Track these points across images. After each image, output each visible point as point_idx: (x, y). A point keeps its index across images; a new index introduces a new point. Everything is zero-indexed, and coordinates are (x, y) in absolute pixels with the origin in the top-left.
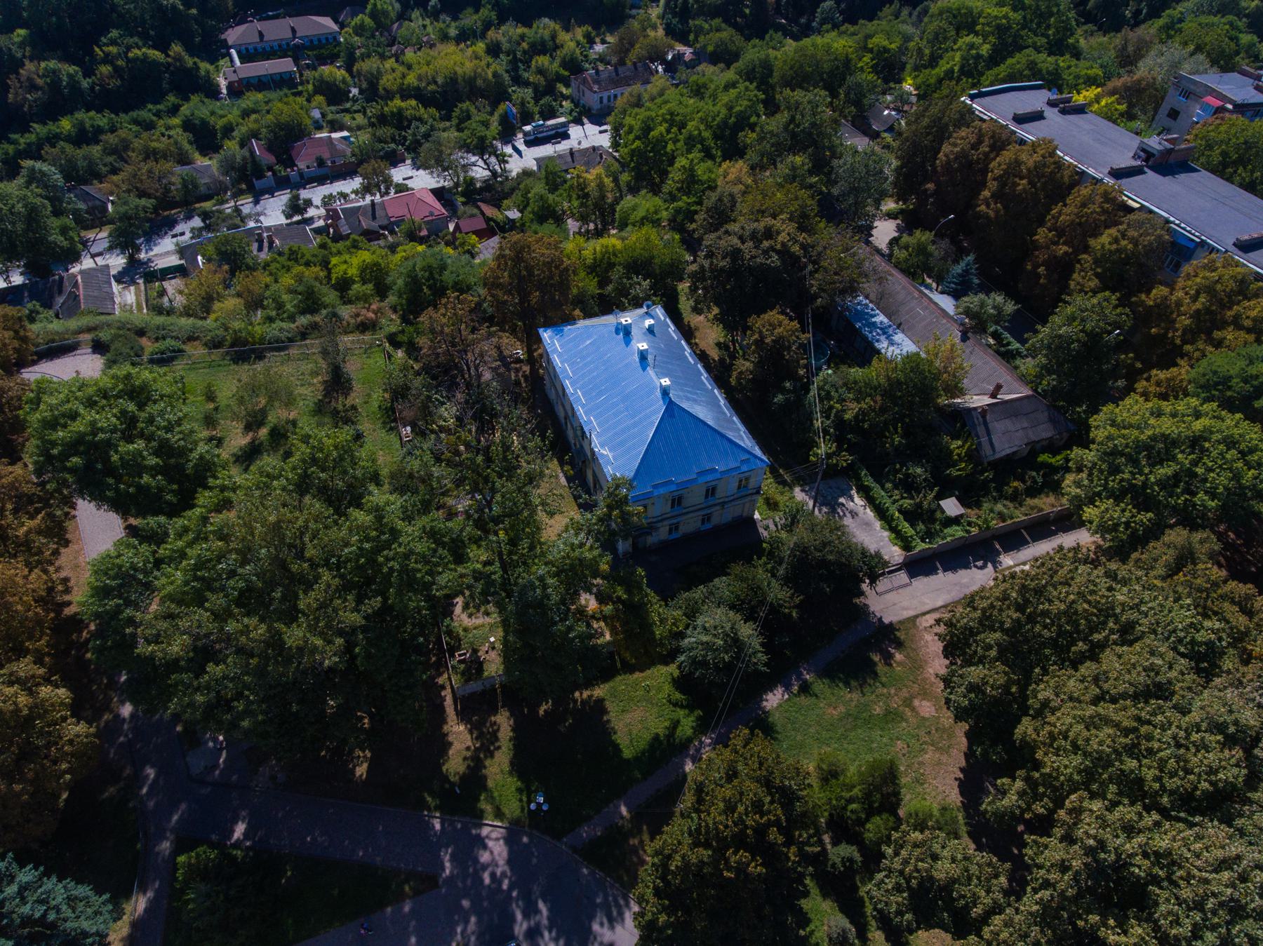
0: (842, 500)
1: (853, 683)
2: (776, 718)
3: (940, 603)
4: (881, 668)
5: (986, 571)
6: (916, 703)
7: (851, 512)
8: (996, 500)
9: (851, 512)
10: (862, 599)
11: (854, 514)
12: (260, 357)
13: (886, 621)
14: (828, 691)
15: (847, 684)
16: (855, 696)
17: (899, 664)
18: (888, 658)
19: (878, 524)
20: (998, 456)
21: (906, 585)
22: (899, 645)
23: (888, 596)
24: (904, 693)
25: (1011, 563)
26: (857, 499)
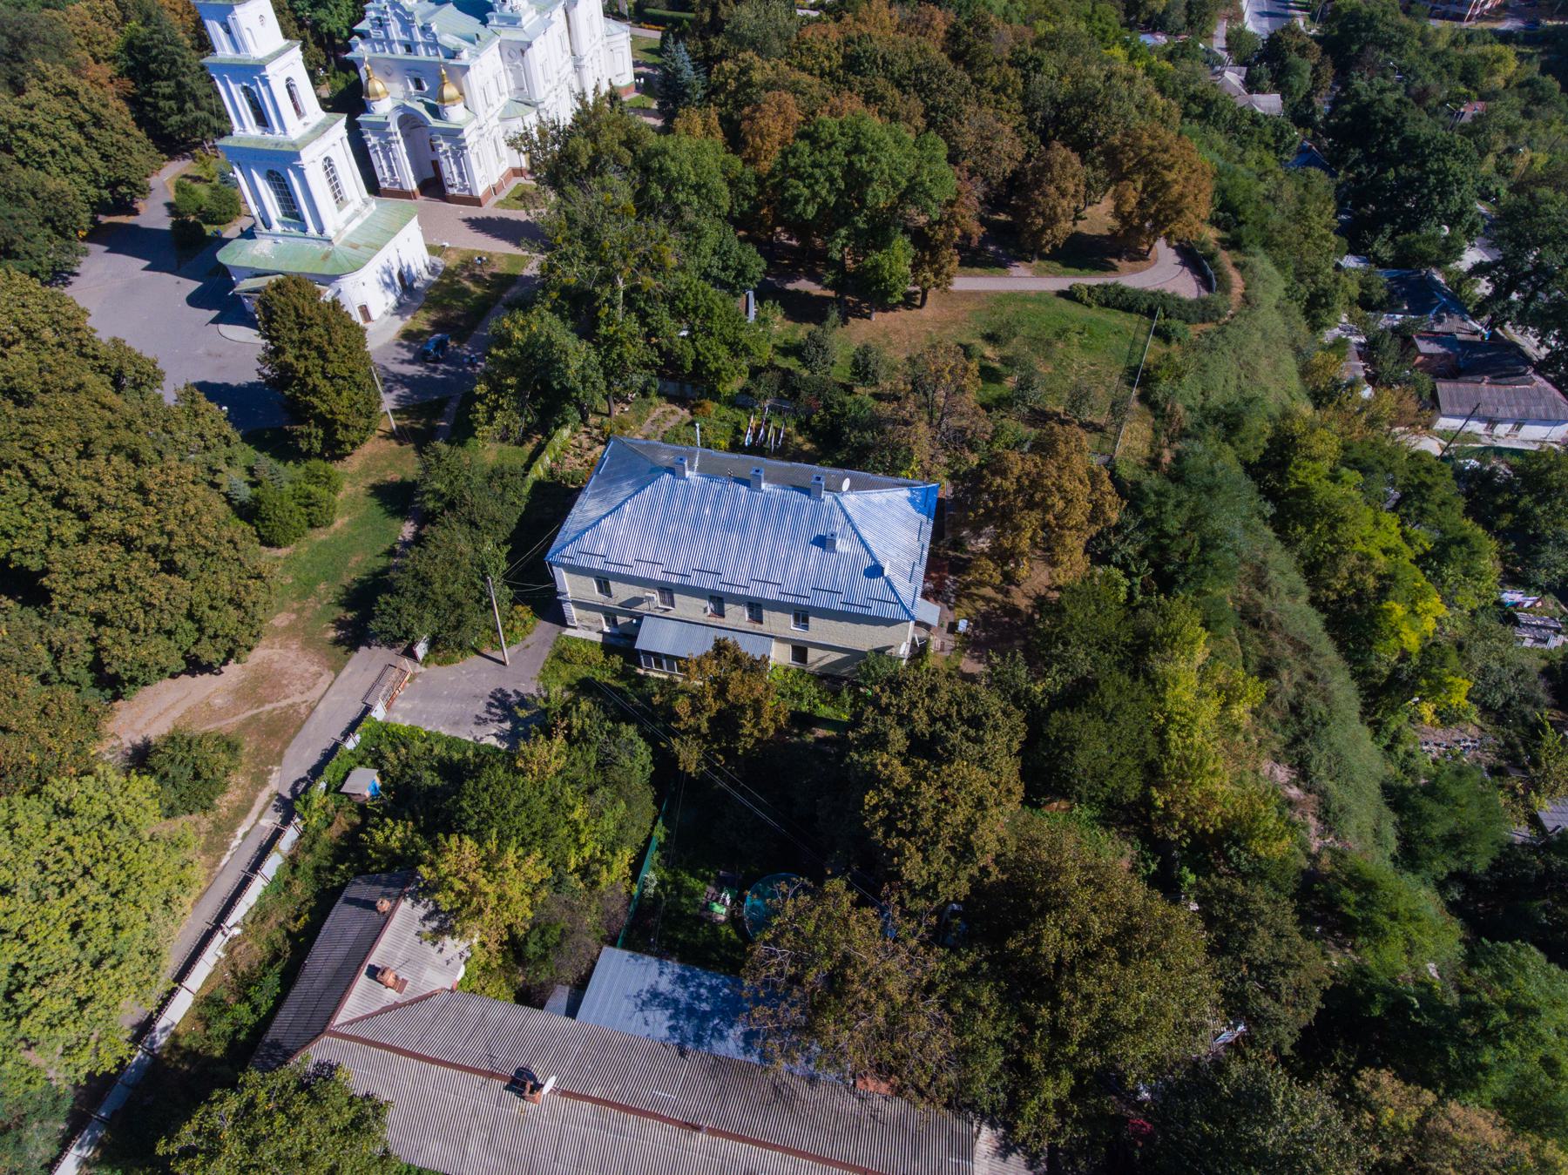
0: (507, 725)
1: (356, 586)
2: (396, 522)
3: (321, 706)
4: (340, 612)
5: (290, 785)
6: (294, 616)
7: (485, 721)
8: (317, 869)
9: (485, 721)
10: (400, 650)
11: (480, 721)
12: (1131, 384)
13: (363, 649)
14: (371, 565)
15: (361, 582)
16: (346, 581)
17: (327, 629)
18: (340, 624)
19: (445, 732)
20: (340, 901)
21: (366, 696)
22: (337, 642)
23: (378, 671)
24: (307, 614)
25: (263, 822)
26: (493, 741)
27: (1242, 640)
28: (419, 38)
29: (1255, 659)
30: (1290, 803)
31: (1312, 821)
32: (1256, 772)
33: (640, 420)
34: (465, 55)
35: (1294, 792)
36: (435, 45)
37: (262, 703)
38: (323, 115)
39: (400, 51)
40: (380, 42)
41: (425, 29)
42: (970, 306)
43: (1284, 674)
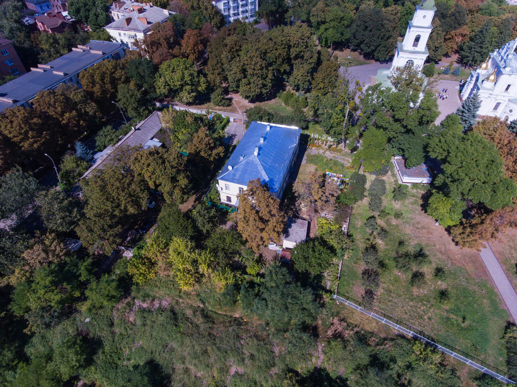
27: (224, 315)
28: (505, 58)
29: (214, 316)
30: (153, 300)
31: (145, 305)
32: (168, 295)
33: (343, 155)
34: (508, 69)
35: (157, 305)
36: (505, 62)
37: (240, 108)
38: (423, 50)
39: (500, 59)
40: (499, 53)
41: (508, 56)
42: (470, 268)
43: (201, 320)
